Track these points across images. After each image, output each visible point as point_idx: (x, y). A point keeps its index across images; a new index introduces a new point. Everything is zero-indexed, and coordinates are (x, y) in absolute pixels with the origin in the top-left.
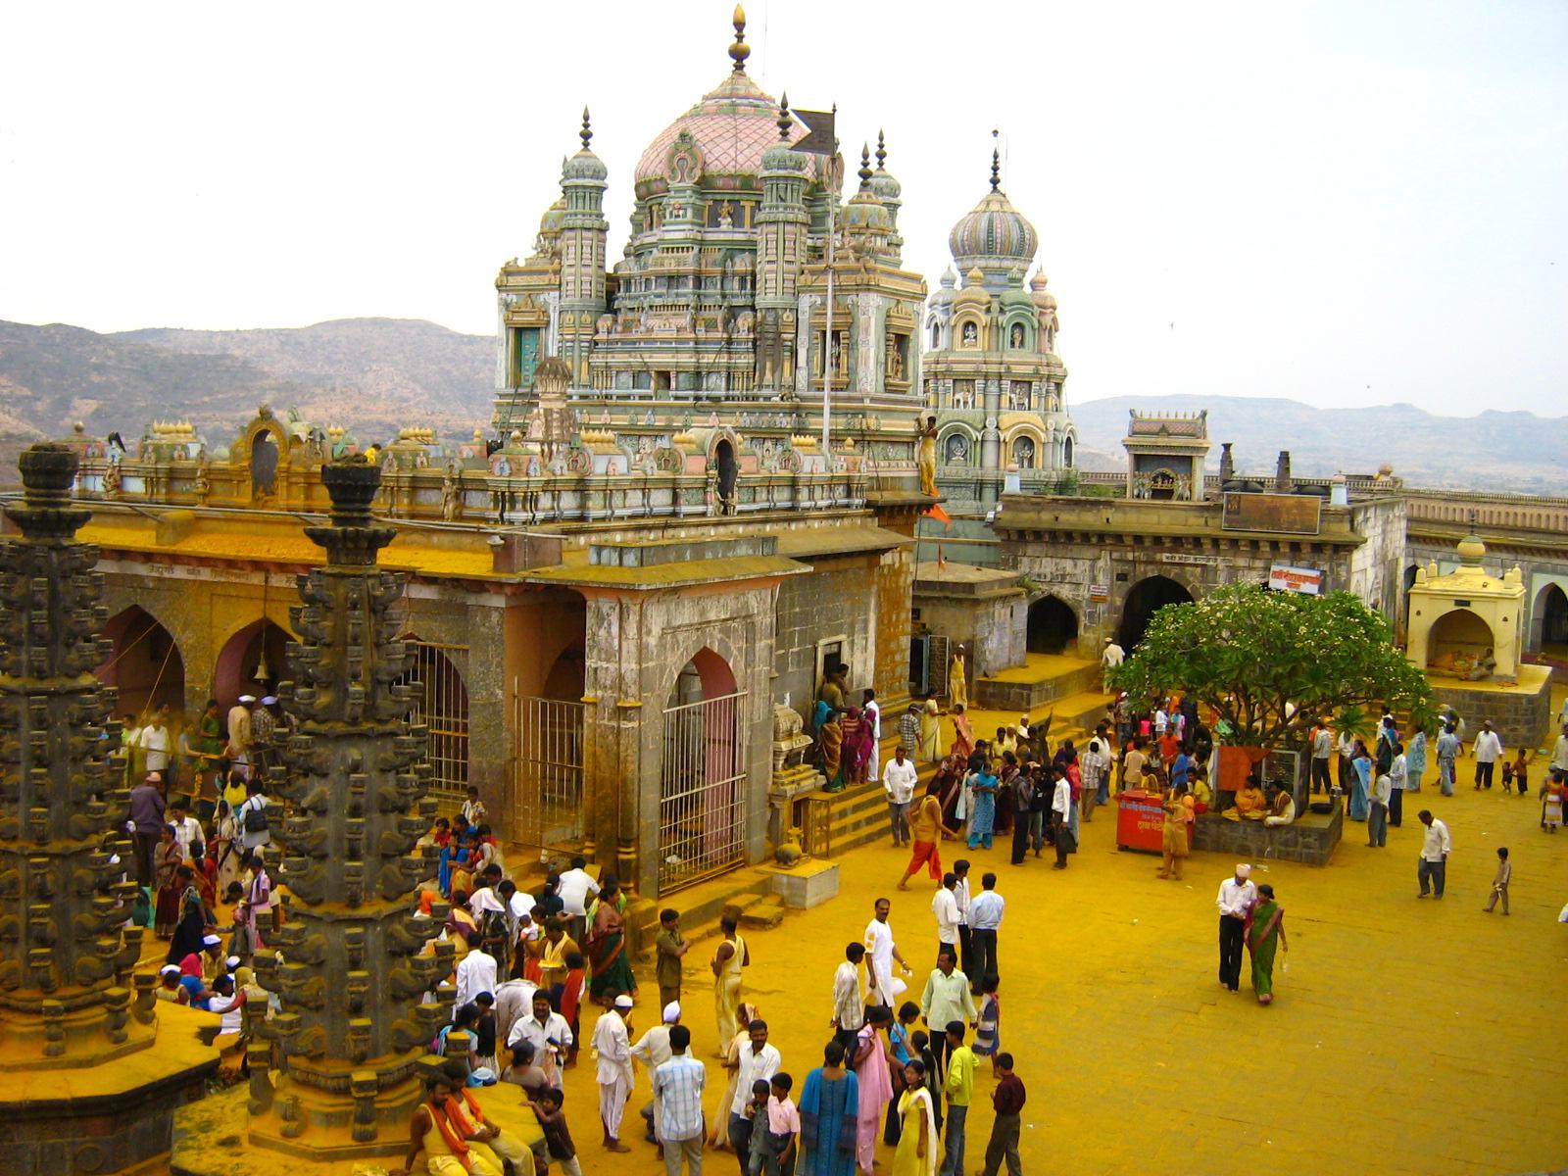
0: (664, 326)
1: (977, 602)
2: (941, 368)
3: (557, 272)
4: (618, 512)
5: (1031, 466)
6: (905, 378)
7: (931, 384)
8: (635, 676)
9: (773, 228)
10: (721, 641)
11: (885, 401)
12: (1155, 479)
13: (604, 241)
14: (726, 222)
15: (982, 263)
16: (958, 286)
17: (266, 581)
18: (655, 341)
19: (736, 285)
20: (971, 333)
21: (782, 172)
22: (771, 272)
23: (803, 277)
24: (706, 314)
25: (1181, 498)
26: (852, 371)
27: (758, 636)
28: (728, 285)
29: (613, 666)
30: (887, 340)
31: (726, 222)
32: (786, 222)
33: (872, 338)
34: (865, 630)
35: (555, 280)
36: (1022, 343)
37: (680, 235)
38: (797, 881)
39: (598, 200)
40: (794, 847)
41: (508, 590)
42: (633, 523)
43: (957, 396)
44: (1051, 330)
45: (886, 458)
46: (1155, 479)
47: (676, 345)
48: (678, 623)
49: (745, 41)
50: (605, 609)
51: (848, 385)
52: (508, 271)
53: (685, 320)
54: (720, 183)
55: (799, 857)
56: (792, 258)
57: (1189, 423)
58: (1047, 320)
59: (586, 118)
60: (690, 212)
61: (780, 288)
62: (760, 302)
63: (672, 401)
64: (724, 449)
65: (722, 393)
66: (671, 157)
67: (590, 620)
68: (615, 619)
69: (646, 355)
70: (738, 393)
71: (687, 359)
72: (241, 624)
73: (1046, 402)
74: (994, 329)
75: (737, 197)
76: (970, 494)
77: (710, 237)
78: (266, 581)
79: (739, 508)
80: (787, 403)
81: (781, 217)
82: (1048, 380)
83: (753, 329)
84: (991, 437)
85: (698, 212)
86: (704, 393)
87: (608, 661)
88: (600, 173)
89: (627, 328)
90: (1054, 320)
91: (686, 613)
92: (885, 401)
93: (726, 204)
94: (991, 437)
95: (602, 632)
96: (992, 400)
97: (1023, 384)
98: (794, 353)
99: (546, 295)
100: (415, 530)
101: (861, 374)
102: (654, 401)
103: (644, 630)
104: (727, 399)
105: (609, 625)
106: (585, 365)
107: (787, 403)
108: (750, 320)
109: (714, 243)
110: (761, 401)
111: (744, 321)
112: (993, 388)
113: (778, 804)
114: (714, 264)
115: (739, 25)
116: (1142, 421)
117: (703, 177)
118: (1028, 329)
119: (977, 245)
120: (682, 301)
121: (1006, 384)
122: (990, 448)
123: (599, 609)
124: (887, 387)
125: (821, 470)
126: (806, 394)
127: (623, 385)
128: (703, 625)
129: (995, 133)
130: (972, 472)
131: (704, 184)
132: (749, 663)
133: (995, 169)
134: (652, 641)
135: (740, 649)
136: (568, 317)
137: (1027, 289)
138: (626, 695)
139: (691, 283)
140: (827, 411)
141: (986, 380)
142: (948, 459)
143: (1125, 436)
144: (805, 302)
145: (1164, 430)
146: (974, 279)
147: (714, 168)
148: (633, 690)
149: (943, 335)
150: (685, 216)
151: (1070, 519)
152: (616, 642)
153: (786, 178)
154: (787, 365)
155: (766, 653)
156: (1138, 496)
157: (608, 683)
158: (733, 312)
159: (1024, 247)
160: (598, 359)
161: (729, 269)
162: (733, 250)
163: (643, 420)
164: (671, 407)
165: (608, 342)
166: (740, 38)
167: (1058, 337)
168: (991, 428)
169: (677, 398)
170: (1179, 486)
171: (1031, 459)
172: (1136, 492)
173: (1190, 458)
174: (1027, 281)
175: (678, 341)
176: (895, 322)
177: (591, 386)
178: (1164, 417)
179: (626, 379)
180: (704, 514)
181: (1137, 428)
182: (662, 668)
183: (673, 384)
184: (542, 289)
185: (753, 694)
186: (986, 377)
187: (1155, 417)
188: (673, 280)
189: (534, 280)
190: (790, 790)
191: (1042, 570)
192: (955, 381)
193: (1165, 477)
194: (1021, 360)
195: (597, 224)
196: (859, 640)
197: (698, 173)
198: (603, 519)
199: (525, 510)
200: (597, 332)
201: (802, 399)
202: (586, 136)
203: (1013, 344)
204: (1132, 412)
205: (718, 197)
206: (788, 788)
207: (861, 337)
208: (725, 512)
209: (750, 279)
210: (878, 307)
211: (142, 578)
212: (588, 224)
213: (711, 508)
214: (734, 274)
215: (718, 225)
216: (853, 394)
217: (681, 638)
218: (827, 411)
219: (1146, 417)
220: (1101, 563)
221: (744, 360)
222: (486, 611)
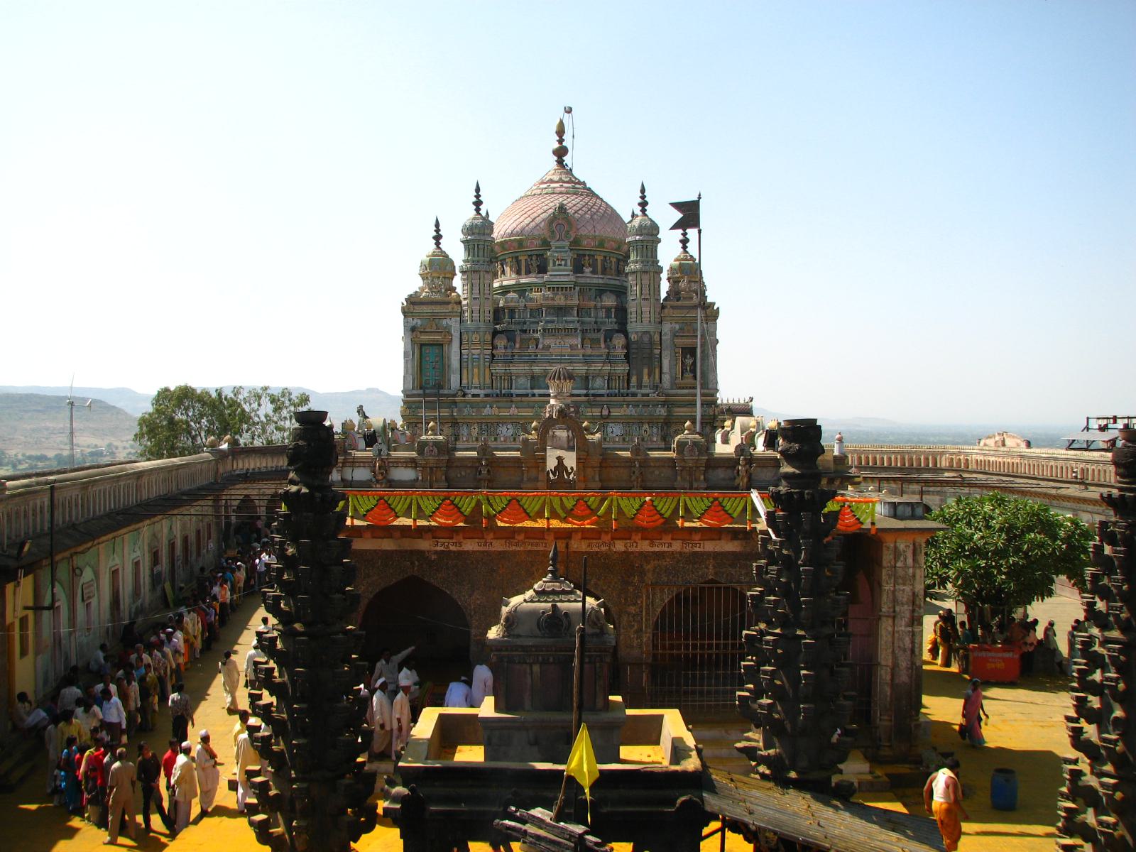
23: (666, 310)
24: (589, 335)
29: (908, 588)
31: (588, 270)
49: (564, 144)
50: (902, 547)
53: (577, 341)
54: (585, 242)
57: (743, 405)
62: (630, 328)
67: (887, 558)
75: (592, 253)
83: (627, 346)
87: (904, 584)
93: (587, 258)
95: (899, 564)
99: (448, 321)
105: (905, 559)
110: (639, 397)
111: (619, 341)
114: (590, 299)
115: (561, 132)
120: (571, 326)
123: (896, 547)
138: (920, 607)
144: (667, 328)
150: (565, 265)
154: (657, 371)
157: (905, 600)
158: (609, 336)
161: (599, 305)
162: (601, 291)
166: (561, 141)
184: (446, 315)
189: (438, 309)
197: (573, 236)
200: (494, 347)
205: (581, 252)
211: (422, 552)
214: (602, 308)
221: (622, 369)
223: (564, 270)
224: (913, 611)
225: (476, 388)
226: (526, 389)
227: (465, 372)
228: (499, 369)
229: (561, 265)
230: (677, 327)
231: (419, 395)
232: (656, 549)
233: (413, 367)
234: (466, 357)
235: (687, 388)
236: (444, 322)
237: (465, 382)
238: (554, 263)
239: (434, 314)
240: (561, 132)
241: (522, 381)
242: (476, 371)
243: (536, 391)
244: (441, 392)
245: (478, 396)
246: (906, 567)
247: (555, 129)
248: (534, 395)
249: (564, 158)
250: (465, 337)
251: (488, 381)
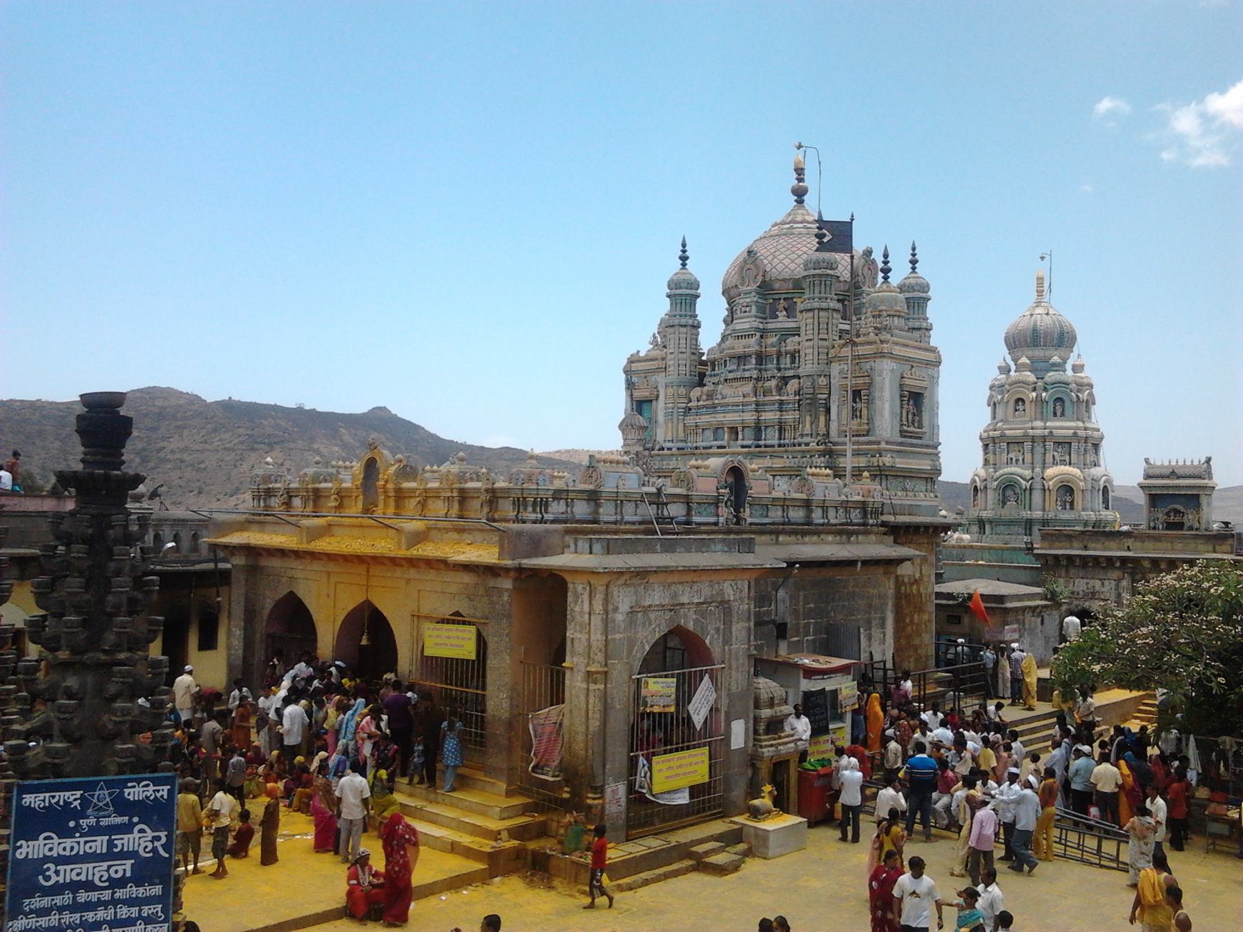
0: (732, 393)
1: (1006, 611)
4: (627, 518)
5: (1072, 508)
6: (920, 427)
7: (991, 447)
8: (601, 645)
9: (811, 314)
10: (696, 621)
11: (901, 444)
12: (1168, 514)
13: (698, 334)
14: (782, 315)
15: (1030, 353)
16: (1012, 373)
19: (788, 360)
20: (1021, 408)
22: (808, 347)
25: (1191, 528)
26: (870, 420)
27: (735, 619)
28: (782, 360)
30: (901, 396)
31: (782, 315)
32: (820, 309)
33: (887, 395)
34: (883, 626)
36: (1063, 414)
37: (747, 326)
38: (760, 833)
39: (692, 305)
40: (765, 802)
41: (512, 574)
42: (642, 527)
43: (1011, 455)
44: (1090, 402)
45: (905, 489)
46: (1168, 514)
47: (741, 407)
48: (647, 603)
50: (580, 588)
51: (868, 431)
52: (631, 361)
53: (748, 388)
54: (777, 286)
55: (769, 812)
56: (825, 336)
58: (1084, 396)
59: (684, 245)
60: (754, 308)
61: (816, 361)
63: (740, 449)
64: (736, 473)
65: (776, 442)
66: (742, 268)
67: (570, 599)
68: (586, 597)
70: (787, 441)
71: (749, 417)
73: (1085, 459)
74: (1039, 404)
76: (1022, 531)
77: (770, 326)
79: (749, 520)
80: (822, 447)
81: (816, 305)
82: (1086, 442)
83: (798, 393)
84: (1038, 486)
85: (761, 309)
86: (762, 443)
88: (694, 285)
90: (1091, 394)
91: (656, 596)
92: (901, 444)
94: (1038, 486)
96: (1038, 457)
97: (1064, 444)
98: (828, 411)
101: (877, 423)
103: (610, 607)
104: (780, 446)
106: (681, 425)
107: (822, 447)
108: (796, 386)
109: (772, 331)
111: (793, 385)
112: (1039, 449)
113: (759, 764)
116: (1154, 467)
117: (764, 282)
118: (1067, 404)
120: (747, 374)
121: (1050, 445)
122: (1037, 496)
124: (903, 433)
125: (833, 496)
126: (837, 440)
127: (707, 439)
128: (675, 607)
130: (1026, 514)
131: (765, 288)
132: (727, 641)
134: (619, 617)
135: (717, 630)
136: (670, 390)
137: (1069, 372)
139: (754, 361)
140: (849, 454)
141: (1033, 441)
142: (1004, 503)
143: (1141, 479)
144: (835, 369)
145: (1173, 474)
146: (1023, 365)
147: (774, 274)
148: (600, 657)
149: (1000, 410)
151: (1097, 550)
152: (587, 616)
153: (820, 275)
154: (822, 419)
155: (744, 633)
156: (1154, 528)
158: (785, 380)
159: (1064, 339)
160: (691, 420)
162: (786, 334)
165: (698, 408)
166: (800, 180)
167: (1095, 409)
168: (1038, 479)
169: (743, 447)
170: (1189, 519)
171: (1072, 503)
172: (1152, 525)
173: (1196, 497)
174: (1069, 366)
176: (907, 382)
177: (685, 441)
178: (1174, 463)
179: (709, 434)
180: (716, 524)
181: (1151, 472)
182: (631, 643)
183: (740, 436)
185: (730, 668)
186: (1033, 439)
187: (1166, 464)
190: (767, 752)
191: (1075, 589)
193: (1177, 512)
194: (1062, 427)
195: (690, 322)
196: (876, 632)
197: (760, 279)
198: (615, 523)
199: (534, 511)
201: (834, 444)
202: (684, 259)
203: (1055, 414)
204: (1147, 461)
206: (765, 750)
207: (877, 394)
208: (738, 523)
209: (794, 355)
210: (892, 371)
212: (683, 321)
213: (721, 520)
215: (777, 317)
216: (870, 438)
217: (652, 616)
218: (849, 454)
219: (1159, 463)
220: (1124, 583)
222: (500, 591)
224: (588, 665)
246: (582, 612)
251: (681, 435)
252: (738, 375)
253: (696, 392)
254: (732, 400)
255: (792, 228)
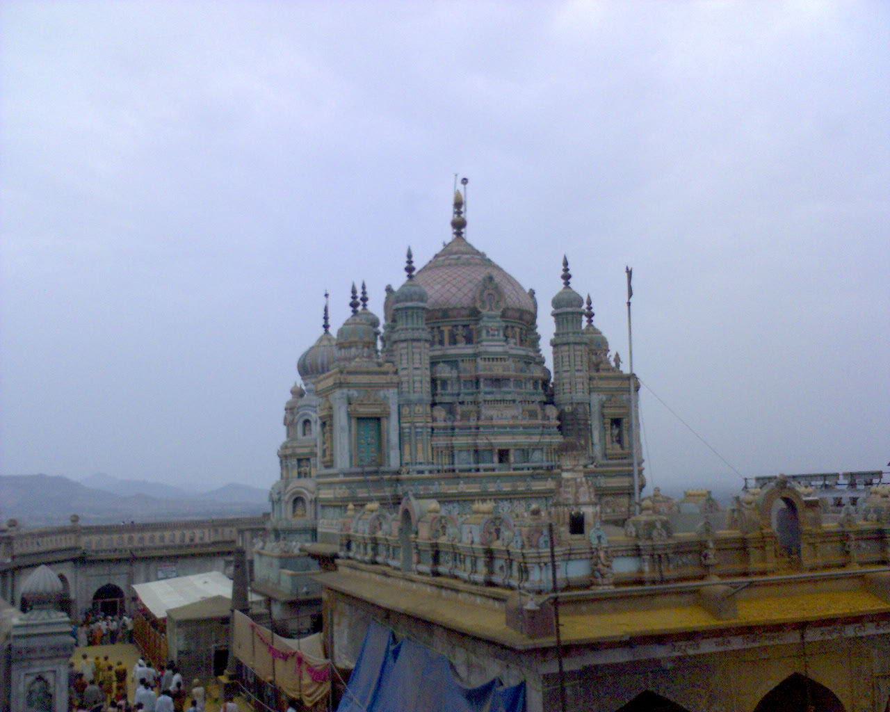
2: (289, 452)
3: (396, 373)
17: (803, 637)
18: (493, 427)
21: (569, 309)
35: (395, 379)
63: (512, 472)
69: (490, 437)
71: (522, 440)
72: (773, 683)
78: (803, 637)
89: (465, 416)
100: (825, 579)
102: (497, 472)
119: (317, 370)
120: (509, 397)
129: (326, 295)
133: (326, 318)
150: (498, 335)
163: (492, 488)
164: (511, 476)
165: (445, 428)
166: (459, 213)
175: (512, 427)
184: (383, 386)
188: (497, 381)
192: (299, 461)
200: (434, 420)
223: (497, 341)
225: (421, 463)
226: (470, 463)
227: (407, 447)
228: (442, 442)
229: (493, 335)
230: (604, 398)
231: (357, 474)
232: (881, 631)
233: (350, 443)
234: (407, 430)
235: (616, 459)
236: (382, 393)
237: (407, 458)
238: (488, 332)
239: (370, 385)
240: (458, 204)
241: (464, 455)
242: (420, 446)
243: (481, 465)
244: (382, 469)
245: (422, 472)
247: (451, 201)
248: (478, 470)
249: (463, 230)
250: (405, 410)
252: (498, 397)
253: (440, 413)
254: (500, 422)
255: (459, 258)
